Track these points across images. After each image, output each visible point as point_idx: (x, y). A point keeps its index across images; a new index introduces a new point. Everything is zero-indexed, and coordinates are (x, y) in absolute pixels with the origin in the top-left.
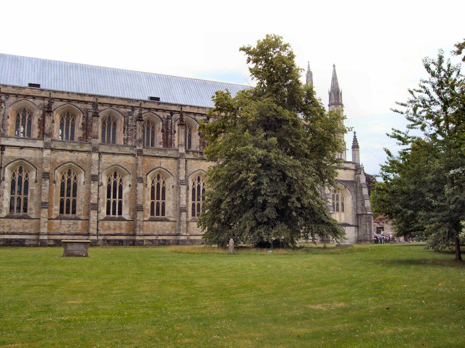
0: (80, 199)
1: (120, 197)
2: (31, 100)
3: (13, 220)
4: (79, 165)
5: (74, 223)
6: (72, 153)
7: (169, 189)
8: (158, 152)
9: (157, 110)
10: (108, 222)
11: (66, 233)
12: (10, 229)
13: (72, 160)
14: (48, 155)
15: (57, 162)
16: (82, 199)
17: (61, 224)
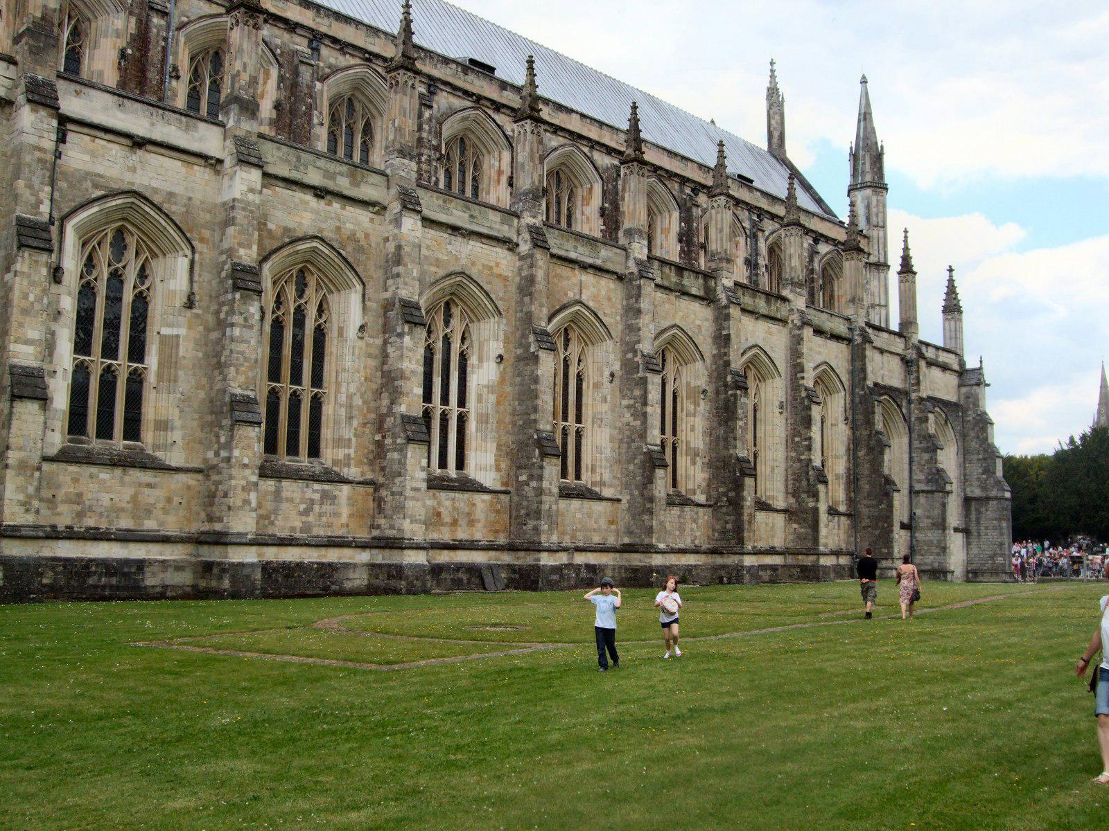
0: (343, 398)
1: (462, 402)
3: (93, 470)
4: (343, 253)
5: (325, 496)
6: (322, 202)
7: (597, 386)
8: (576, 247)
9: (498, 107)
10: (434, 497)
11: (298, 535)
12: (80, 515)
13: (321, 230)
14: (251, 190)
15: (270, 231)
16: (350, 397)
17: (278, 492)
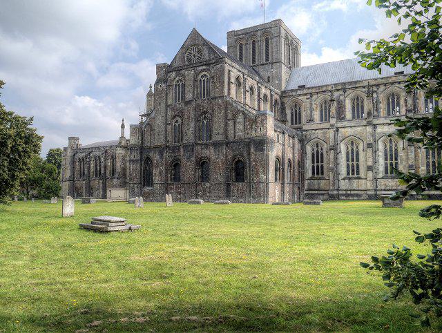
2: (397, 85)
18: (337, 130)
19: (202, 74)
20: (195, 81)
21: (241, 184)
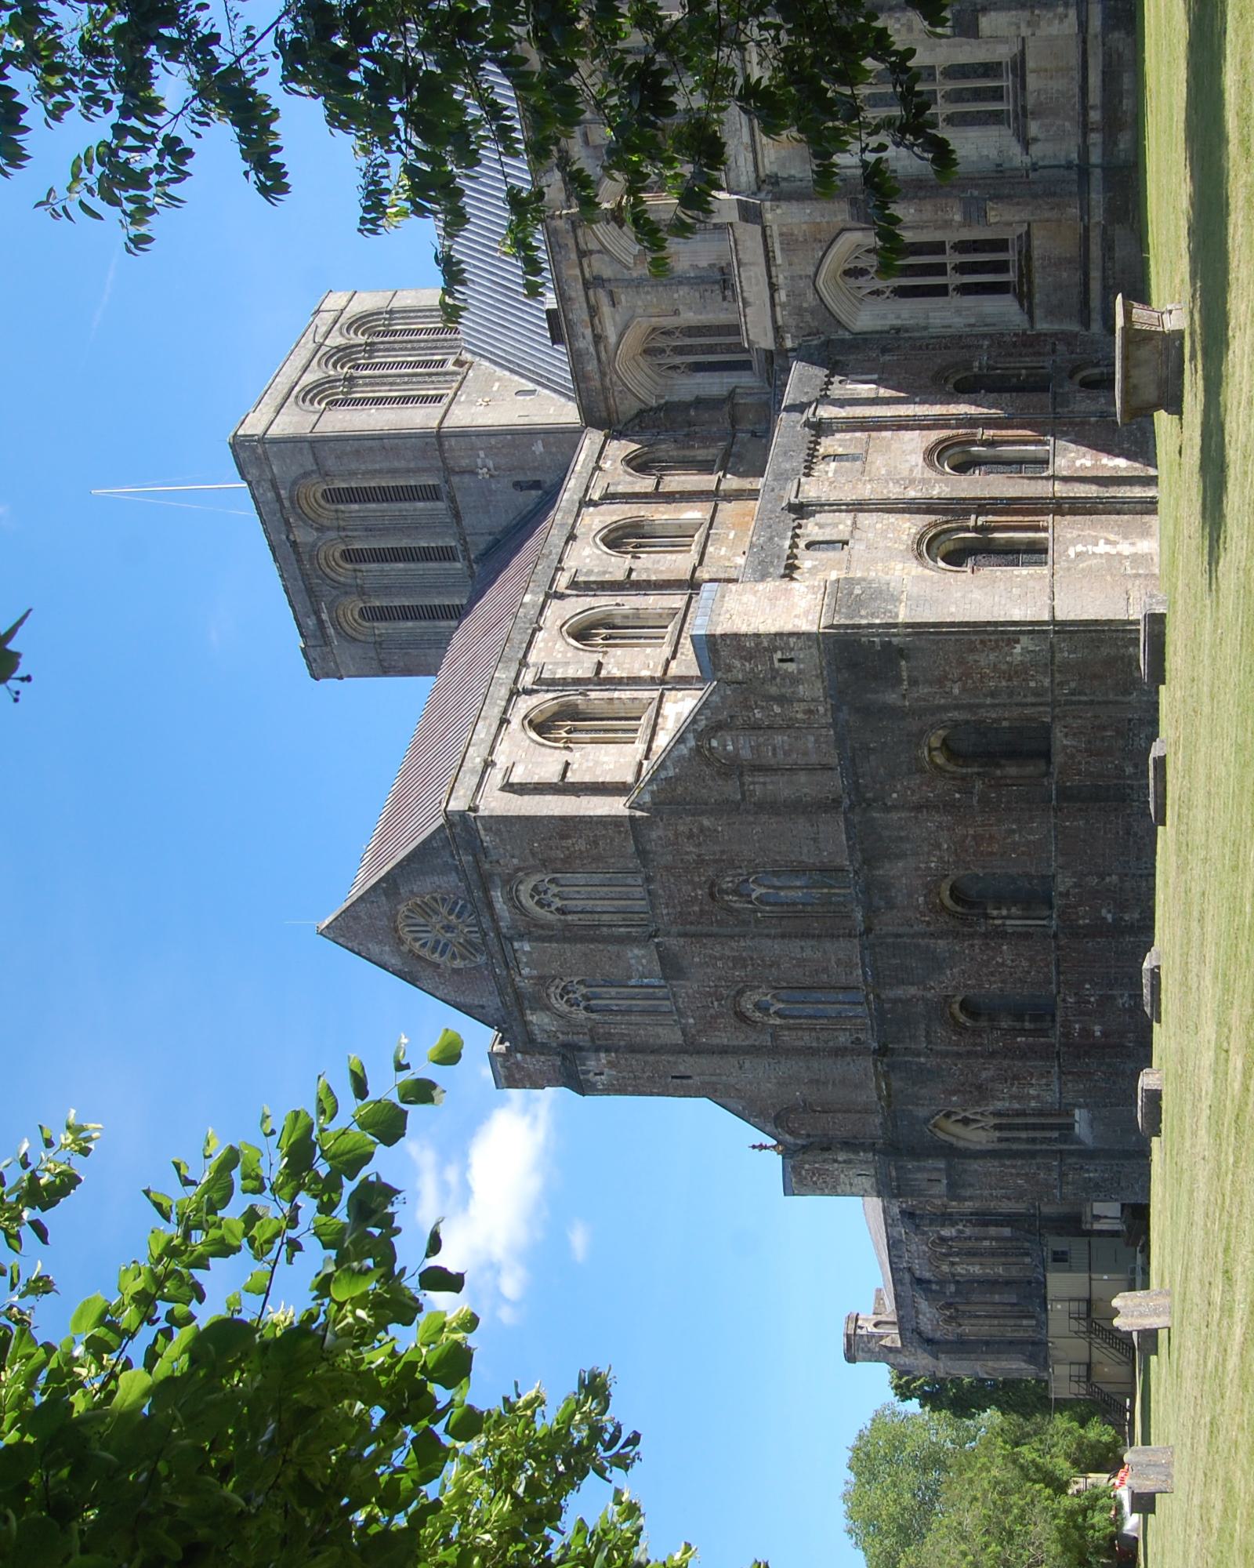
18: (774, 180)
19: (529, 903)
20: (568, 935)
21: (1061, 739)
